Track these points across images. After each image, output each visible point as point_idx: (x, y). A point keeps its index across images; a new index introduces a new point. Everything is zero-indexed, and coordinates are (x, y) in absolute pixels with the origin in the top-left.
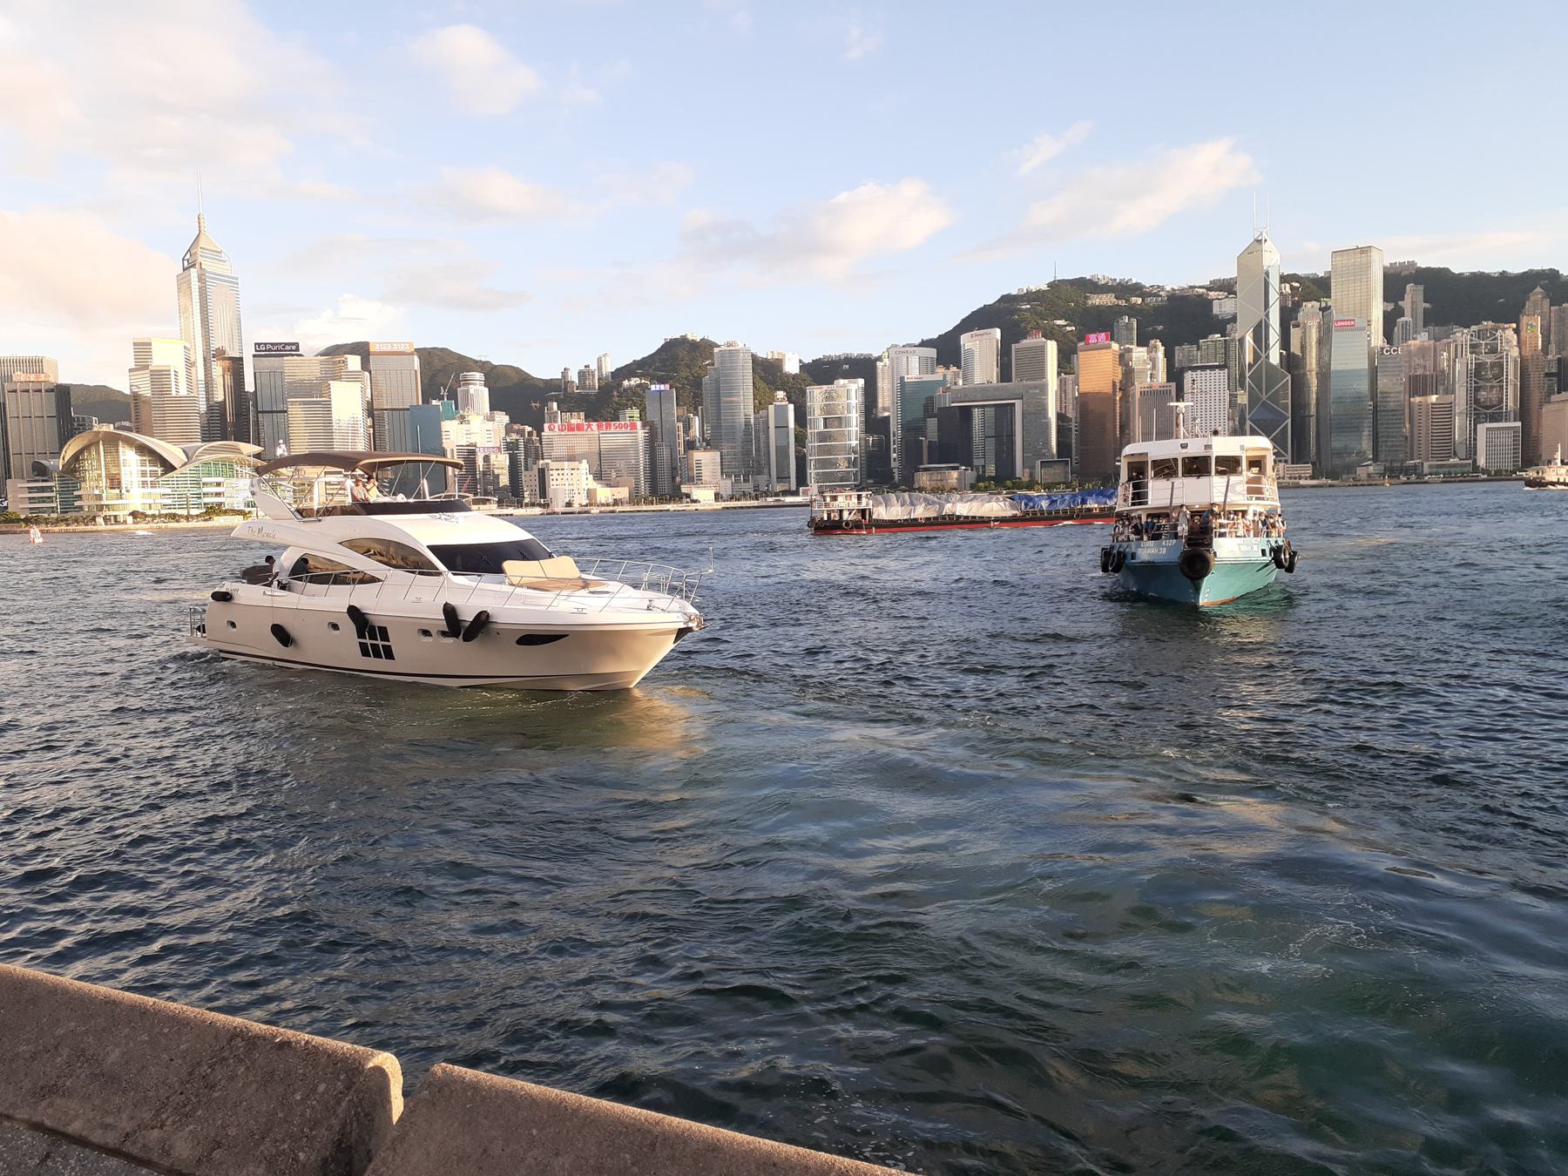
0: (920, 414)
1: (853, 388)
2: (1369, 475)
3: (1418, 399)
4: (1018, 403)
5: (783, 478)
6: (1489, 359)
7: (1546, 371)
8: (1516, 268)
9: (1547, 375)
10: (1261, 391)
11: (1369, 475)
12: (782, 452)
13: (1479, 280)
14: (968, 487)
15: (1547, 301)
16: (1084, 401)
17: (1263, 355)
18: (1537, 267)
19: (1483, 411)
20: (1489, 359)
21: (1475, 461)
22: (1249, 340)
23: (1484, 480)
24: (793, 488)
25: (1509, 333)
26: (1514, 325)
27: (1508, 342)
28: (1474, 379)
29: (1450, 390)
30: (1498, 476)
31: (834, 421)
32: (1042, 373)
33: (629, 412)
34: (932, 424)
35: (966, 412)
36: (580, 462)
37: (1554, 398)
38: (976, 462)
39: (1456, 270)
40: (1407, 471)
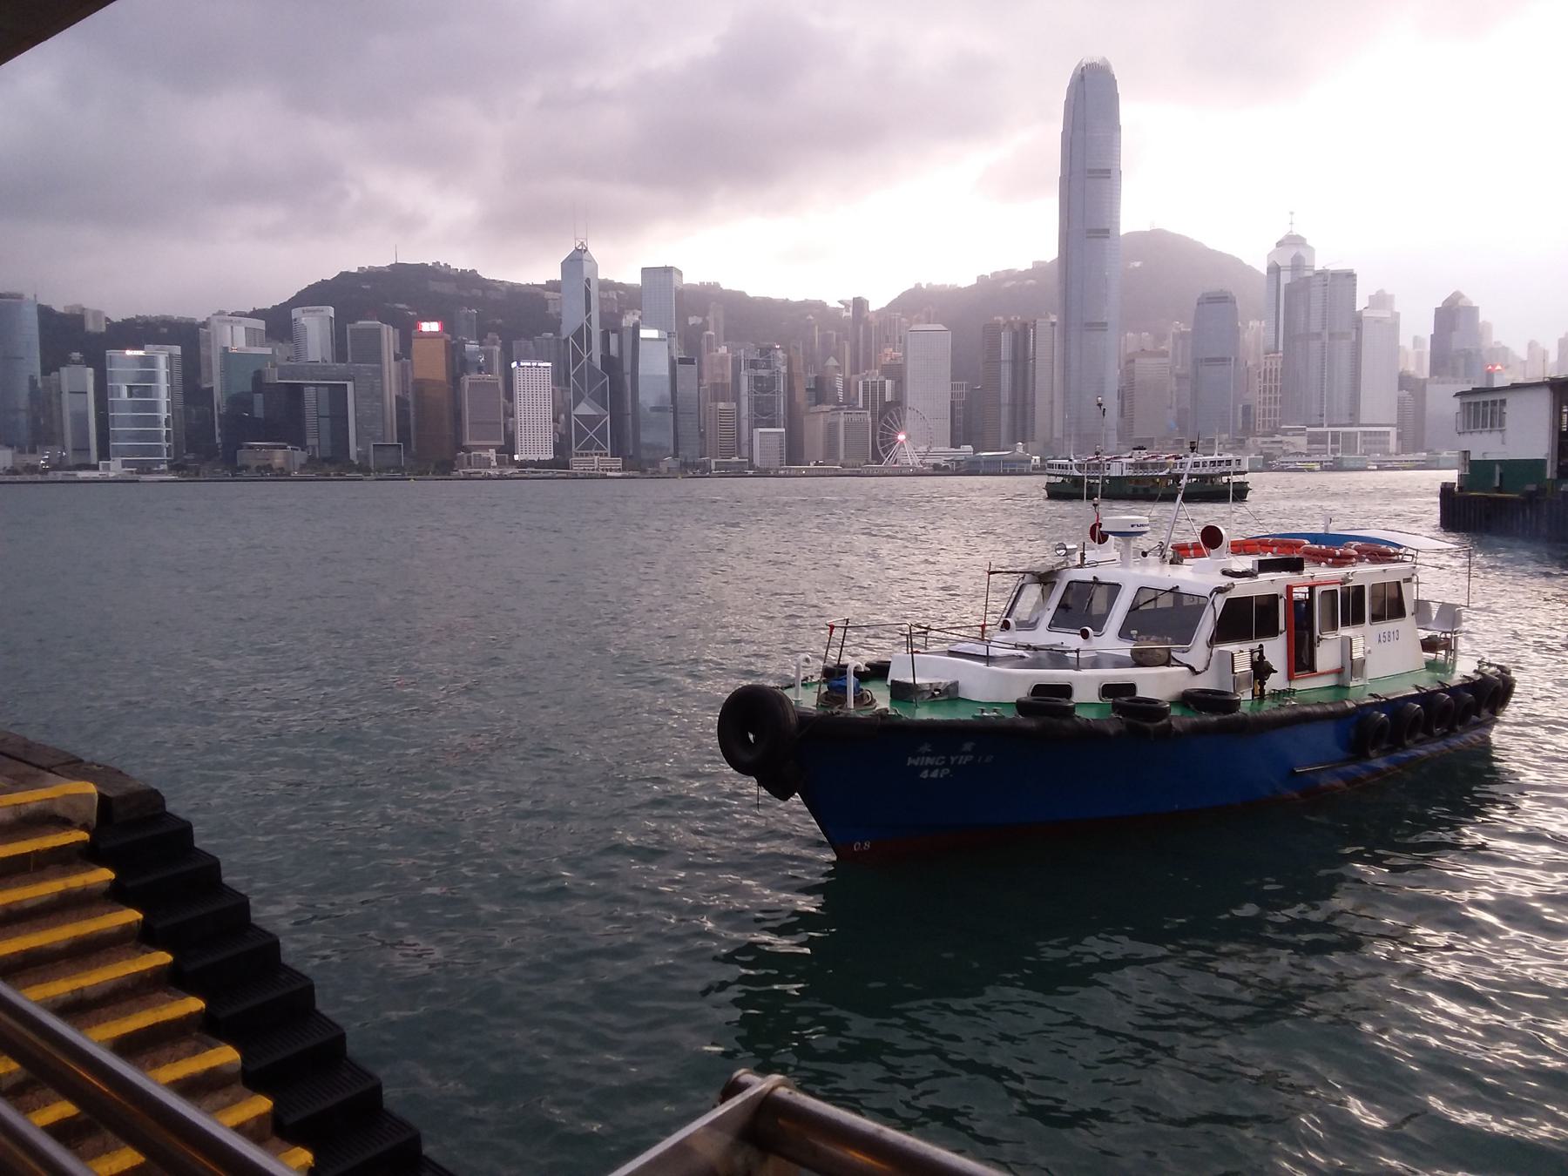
0: (250, 389)
1: (163, 358)
4: (350, 385)
5: (83, 449)
10: (583, 388)
12: (81, 419)
14: (298, 467)
16: (420, 384)
21: (751, 460)
24: (94, 459)
28: (754, 390)
29: (737, 399)
31: (143, 388)
32: (376, 356)
34: (259, 399)
35: (296, 391)
37: (813, 409)
38: (310, 442)
40: (695, 466)
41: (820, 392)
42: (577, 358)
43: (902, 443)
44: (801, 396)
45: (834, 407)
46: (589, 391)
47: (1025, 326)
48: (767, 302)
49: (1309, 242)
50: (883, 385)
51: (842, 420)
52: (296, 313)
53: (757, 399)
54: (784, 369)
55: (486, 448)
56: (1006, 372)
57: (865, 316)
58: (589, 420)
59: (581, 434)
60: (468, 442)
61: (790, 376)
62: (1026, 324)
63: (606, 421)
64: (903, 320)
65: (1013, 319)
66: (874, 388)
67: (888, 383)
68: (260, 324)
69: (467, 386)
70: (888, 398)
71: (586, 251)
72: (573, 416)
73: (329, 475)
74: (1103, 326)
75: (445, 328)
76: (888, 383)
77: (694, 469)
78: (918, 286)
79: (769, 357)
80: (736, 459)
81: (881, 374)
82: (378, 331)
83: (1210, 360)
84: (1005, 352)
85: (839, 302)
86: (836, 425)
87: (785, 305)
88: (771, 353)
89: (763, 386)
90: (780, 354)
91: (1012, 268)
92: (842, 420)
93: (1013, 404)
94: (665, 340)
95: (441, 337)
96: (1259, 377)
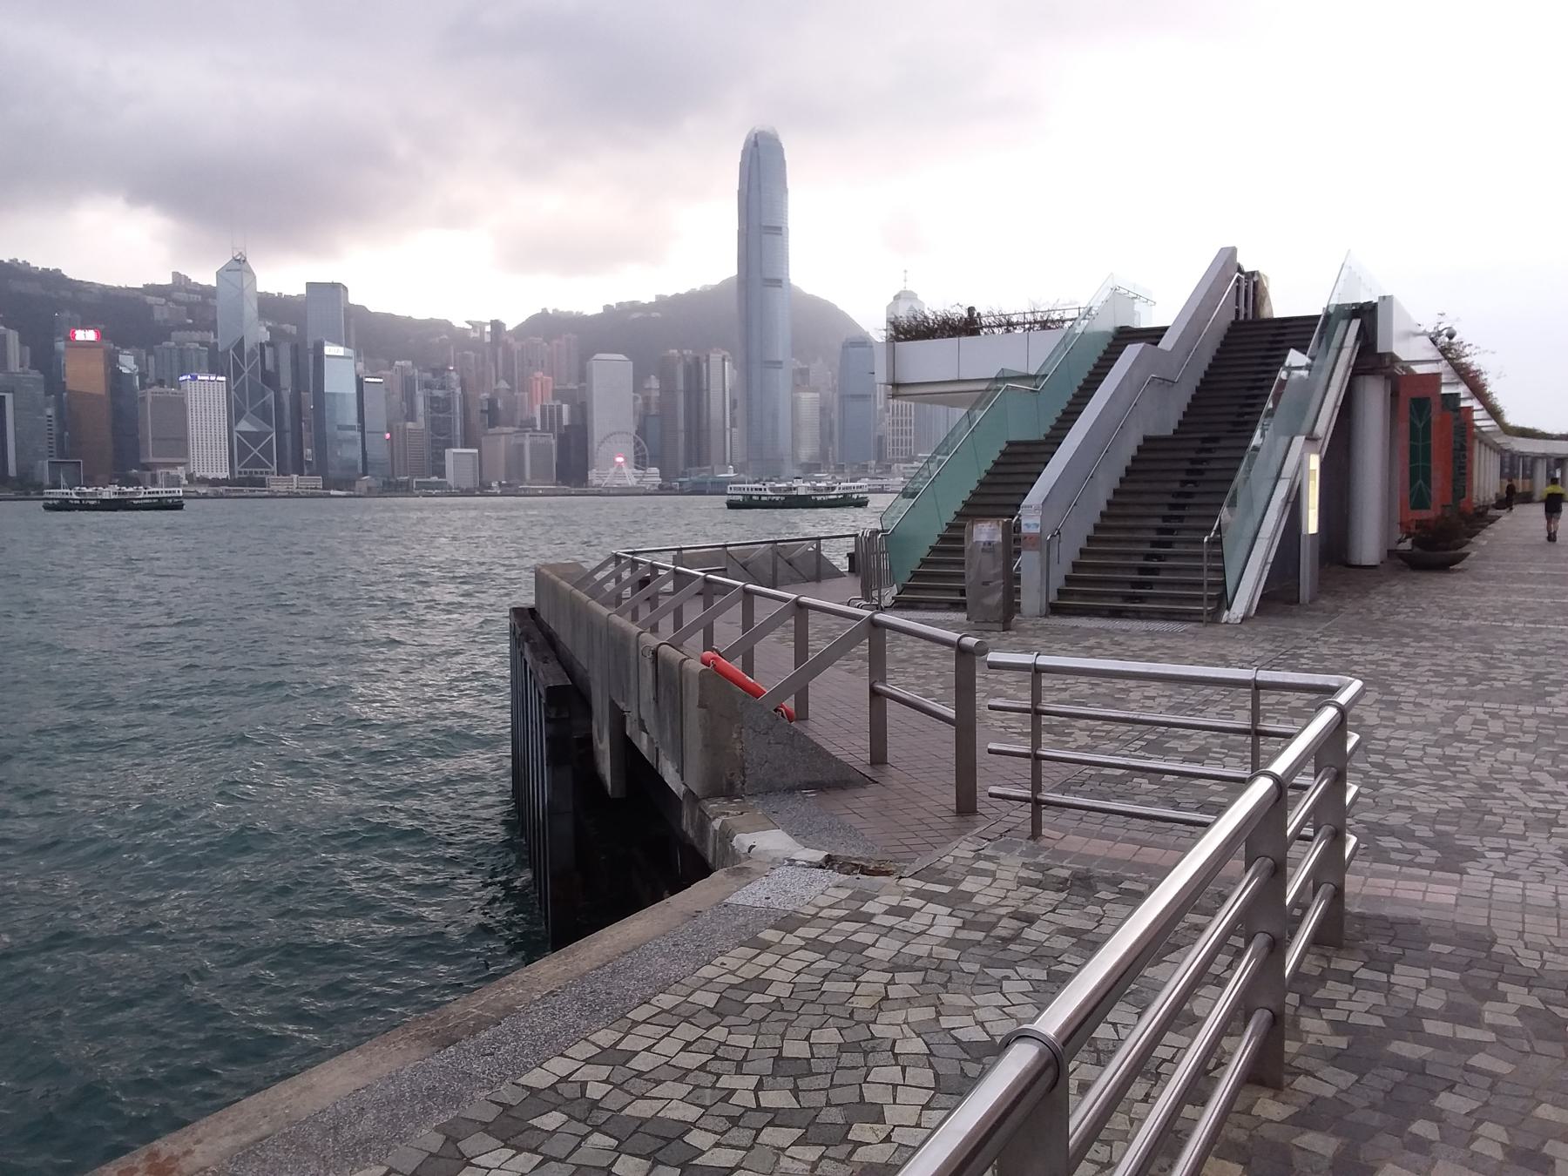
7: (479, 408)
9: (482, 411)
17: (246, 371)
19: (440, 438)
20: (439, 393)
37: (491, 431)
41: (492, 415)
42: (238, 372)
43: (620, 465)
44: (475, 415)
45: (517, 429)
46: (250, 406)
47: (697, 361)
48: (390, 318)
49: (919, 297)
50: (560, 409)
51: (527, 443)
53: (433, 419)
55: (174, 465)
56: (681, 398)
57: (504, 338)
58: (254, 438)
59: (243, 451)
60: (152, 460)
61: (465, 397)
62: (698, 358)
63: (272, 438)
64: (545, 344)
65: (685, 352)
66: (551, 411)
67: (565, 407)
69: (149, 400)
70: (566, 422)
71: (244, 261)
72: (235, 434)
73: (28, 494)
74: (777, 364)
75: (100, 335)
76: (565, 407)
77: (392, 488)
78: (545, 310)
79: (443, 378)
80: (435, 479)
81: (554, 399)
83: (855, 397)
84: (681, 386)
85: (468, 322)
86: (521, 446)
87: (408, 322)
88: (446, 374)
89: (439, 406)
90: (454, 376)
91: (626, 298)
92: (527, 443)
94: (350, 358)
95: (100, 347)
96: (888, 411)
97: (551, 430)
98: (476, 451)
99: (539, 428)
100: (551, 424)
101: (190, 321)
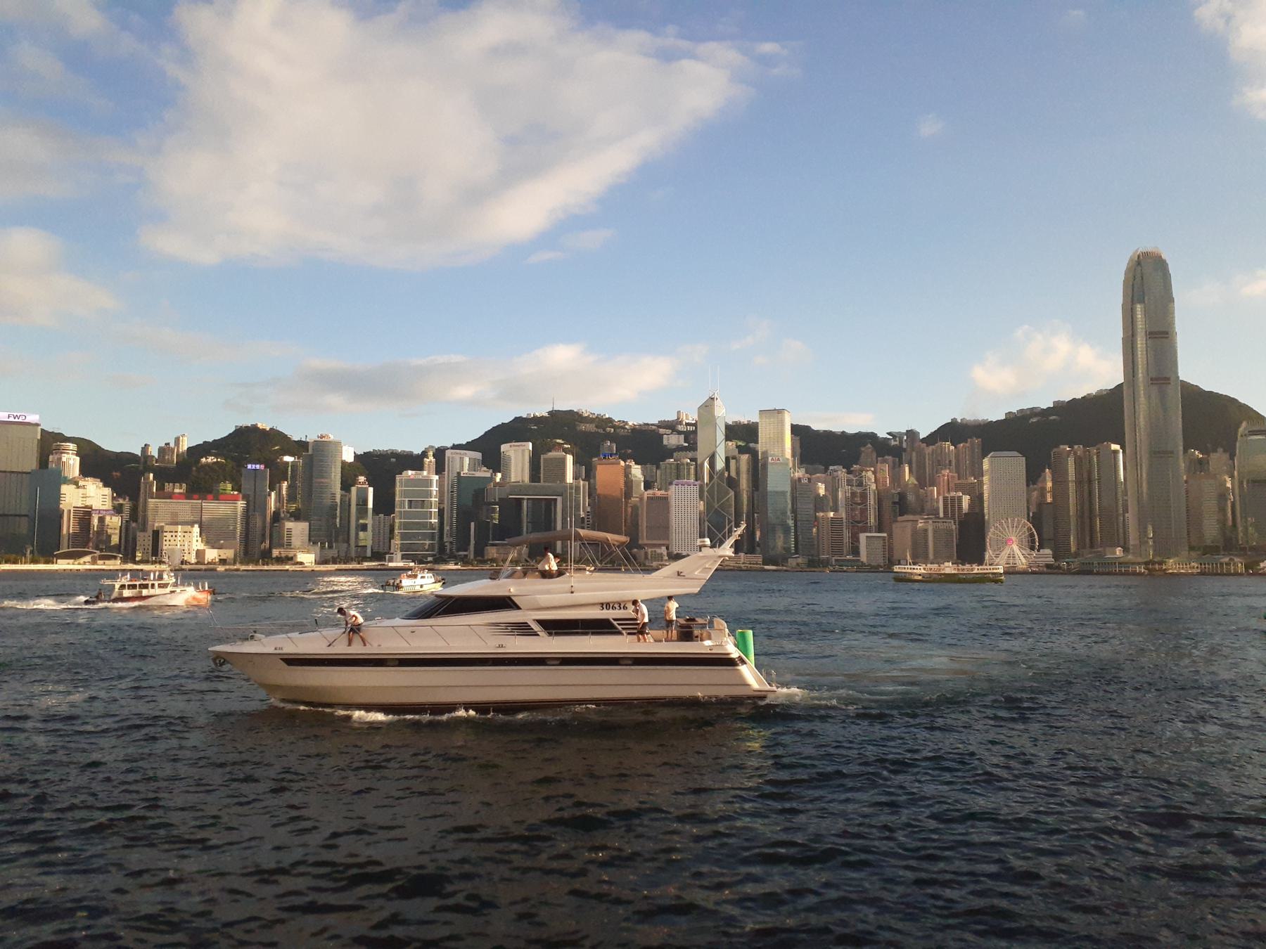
2: (798, 564)
3: (821, 514)
6: (858, 490)
8: (851, 430)
9: (894, 503)
11: (798, 564)
13: (828, 435)
15: (874, 455)
18: (863, 430)
22: (706, 465)
23: (882, 572)
25: (870, 474)
26: (872, 469)
27: (870, 479)
30: (873, 569)
33: (222, 485)
36: (193, 526)
37: (900, 518)
39: (815, 427)
50: (960, 499)
52: (504, 447)
54: (874, 486)
68: (478, 455)
76: (966, 500)
82: (563, 461)
88: (864, 474)
93: (1080, 516)
97: (953, 517)
98: (885, 535)
99: (941, 515)
100: (953, 515)
101: (686, 444)
